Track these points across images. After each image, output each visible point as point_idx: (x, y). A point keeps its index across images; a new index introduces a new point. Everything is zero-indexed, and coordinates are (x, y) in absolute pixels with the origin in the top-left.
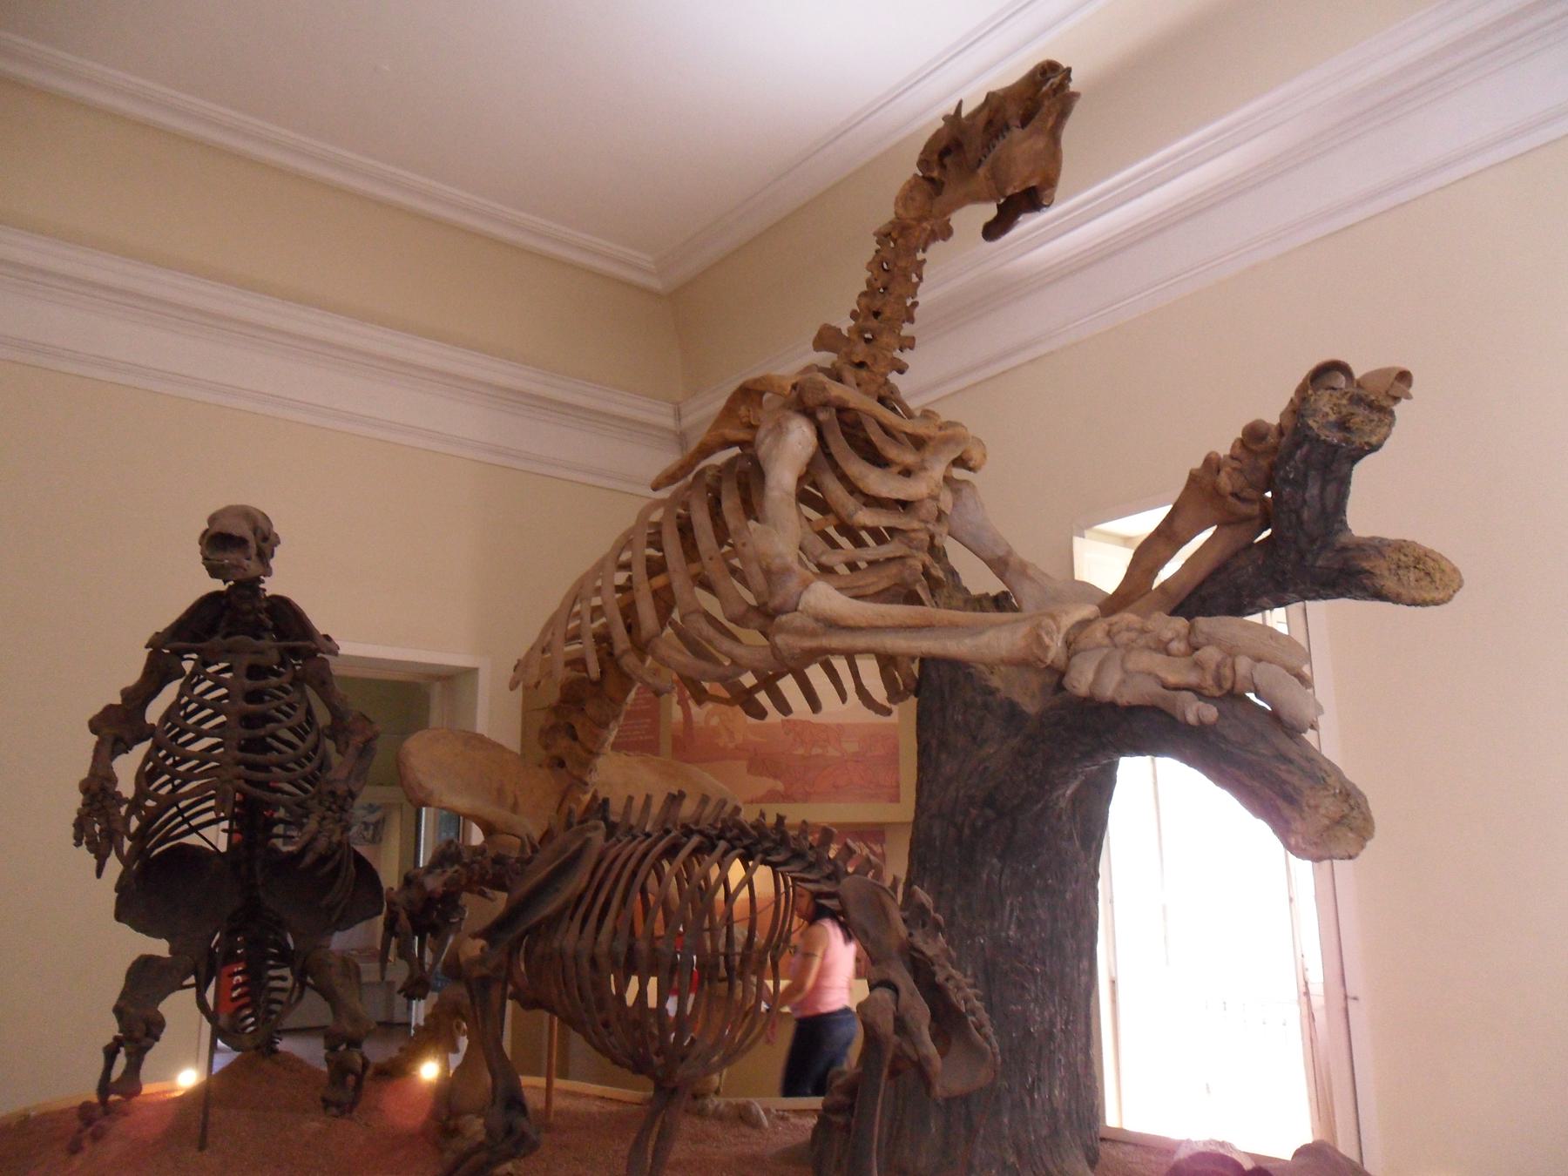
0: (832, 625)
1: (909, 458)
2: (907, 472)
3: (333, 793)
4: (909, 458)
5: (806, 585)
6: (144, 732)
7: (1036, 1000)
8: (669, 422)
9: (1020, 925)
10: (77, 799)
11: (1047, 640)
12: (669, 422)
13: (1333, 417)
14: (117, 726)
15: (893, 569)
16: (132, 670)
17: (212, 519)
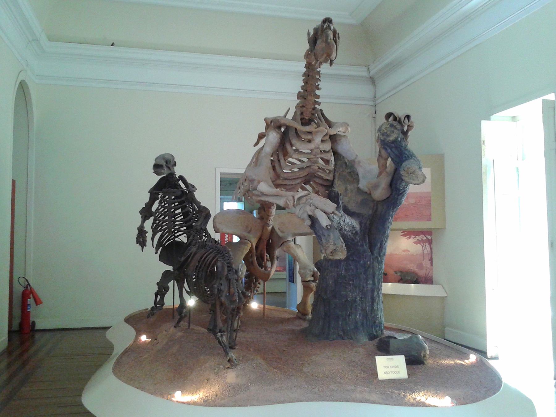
0: (263, 194)
1: (309, 137)
2: (310, 141)
3: (196, 229)
4: (309, 137)
5: (259, 182)
6: (151, 214)
7: (350, 291)
8: (365, 74)
9: (346, 270)
10: (137, 232)
11: (288, 203)
12: (365, 74)
13: (386, 131)
14: (146, 213)
15: (308, 170)
16: (146, 198)
17: (156, 159)
